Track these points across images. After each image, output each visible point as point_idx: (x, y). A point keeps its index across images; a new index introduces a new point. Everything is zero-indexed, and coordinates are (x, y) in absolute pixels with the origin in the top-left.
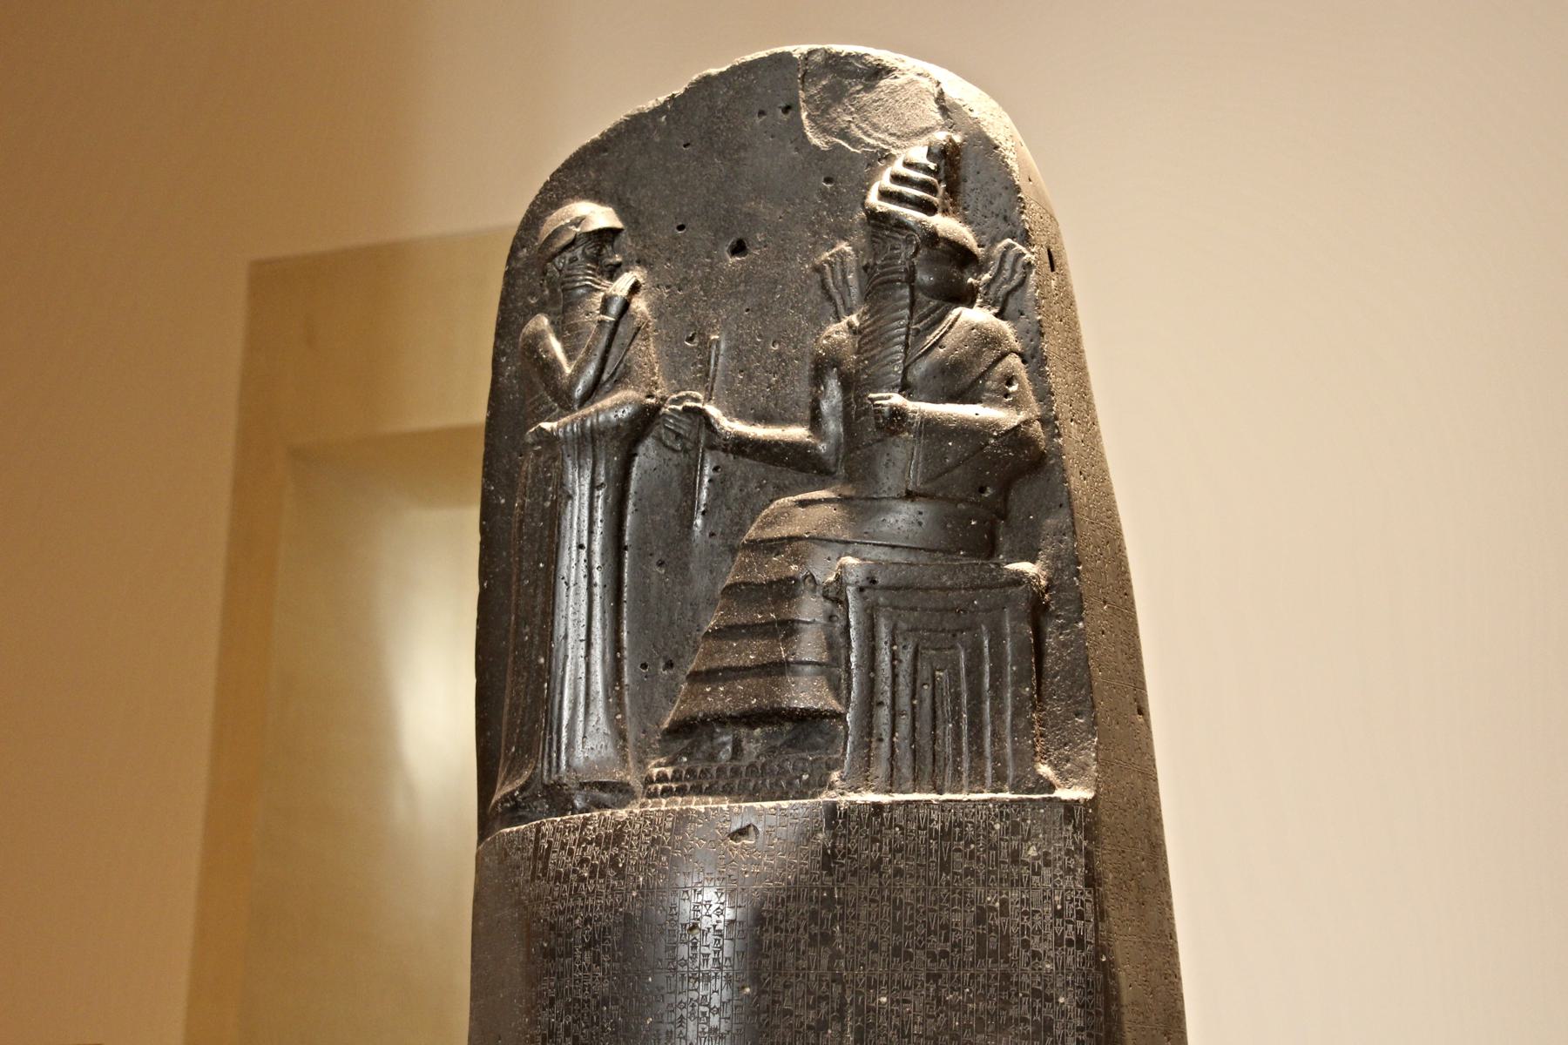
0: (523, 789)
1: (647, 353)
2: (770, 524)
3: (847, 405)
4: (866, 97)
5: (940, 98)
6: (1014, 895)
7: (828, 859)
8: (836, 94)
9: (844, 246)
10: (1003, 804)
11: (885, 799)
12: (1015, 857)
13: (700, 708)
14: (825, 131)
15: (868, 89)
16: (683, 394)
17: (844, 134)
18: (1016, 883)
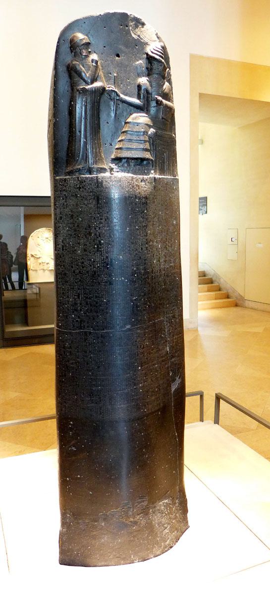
0: (83, 168)
1: (101, 73)
2: (133, 119)
3: (148, 97)
4: (142, 29)
5: (157, 34)
6: (173, 195)
7: (155, 187)
8: (137, 27)
9: (141, 61)
10: (172, 179)
11: (161, 177)
12: (173, 188)
13: (119, 155)
14: (135, 34)
15: (143, 27)
16: (109, 86)
17: (139, 36)
18: (173, 193)
